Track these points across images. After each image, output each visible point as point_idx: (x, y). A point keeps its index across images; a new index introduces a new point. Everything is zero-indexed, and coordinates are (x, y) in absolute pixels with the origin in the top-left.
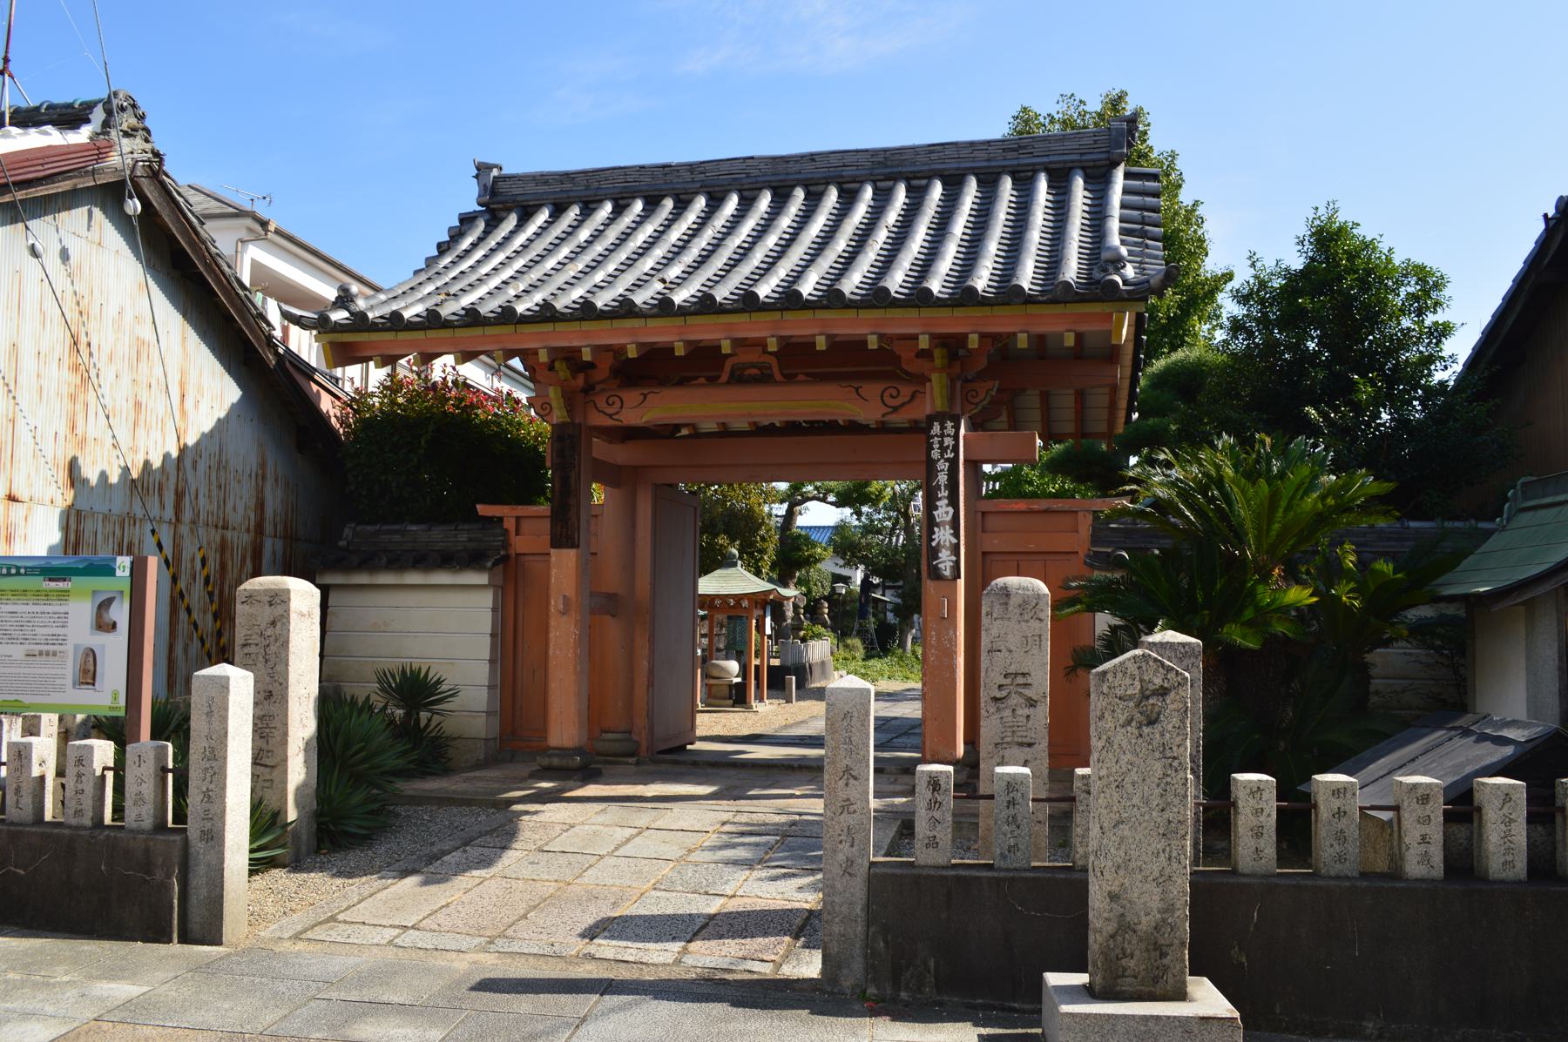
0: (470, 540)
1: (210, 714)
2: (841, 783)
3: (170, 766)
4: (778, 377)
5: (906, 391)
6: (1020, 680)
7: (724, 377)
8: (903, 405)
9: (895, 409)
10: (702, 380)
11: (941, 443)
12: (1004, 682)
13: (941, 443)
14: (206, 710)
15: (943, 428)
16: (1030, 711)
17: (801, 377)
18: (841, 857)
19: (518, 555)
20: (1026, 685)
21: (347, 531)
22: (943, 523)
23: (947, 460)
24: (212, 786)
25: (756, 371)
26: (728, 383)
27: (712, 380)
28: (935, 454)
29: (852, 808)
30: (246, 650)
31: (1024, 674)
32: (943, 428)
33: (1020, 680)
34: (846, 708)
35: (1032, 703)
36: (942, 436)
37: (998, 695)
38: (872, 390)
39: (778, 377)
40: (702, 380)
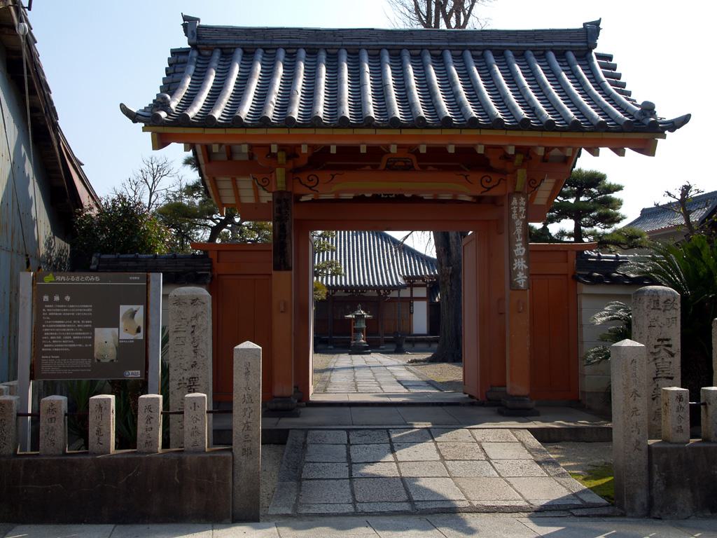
0: (186, 265)
1: (247, 373)
2: (632, 399)
3: (30, 412)
4: (417, 167)
5: (495, 178)
6: (666, 343)
7: (383, 166)
8: (494, 186)
9: (489, 189)
10: (368, 168)
11: (518, 210)
12: (657, 343)
13: (518, 210)
14: (245, 371)
15: (518, 201)
16: (670, 359)
17: (431, 168)
18: (633, 440)
19: (218, 275)
20: (670, 346)
21: (94, 259)
22: (519, 257)
23: (522, 220)
24: (249, 420)
25: (403, 164)
26: (384, 170)
27: (375, 168)
28: (514, 216)
29: (638, 413)
30: (178, 335)
31: (667, 340)
32: (518, 201)
33: (666, 343)
34: (633, 358)
35: (672, 355)
36: (518, 206)
37: (654, 351)
38: (475, 177)
39: (417, 167)
40: (368, 168)
